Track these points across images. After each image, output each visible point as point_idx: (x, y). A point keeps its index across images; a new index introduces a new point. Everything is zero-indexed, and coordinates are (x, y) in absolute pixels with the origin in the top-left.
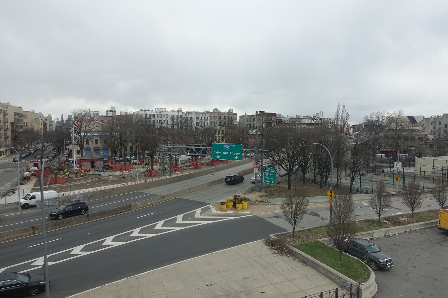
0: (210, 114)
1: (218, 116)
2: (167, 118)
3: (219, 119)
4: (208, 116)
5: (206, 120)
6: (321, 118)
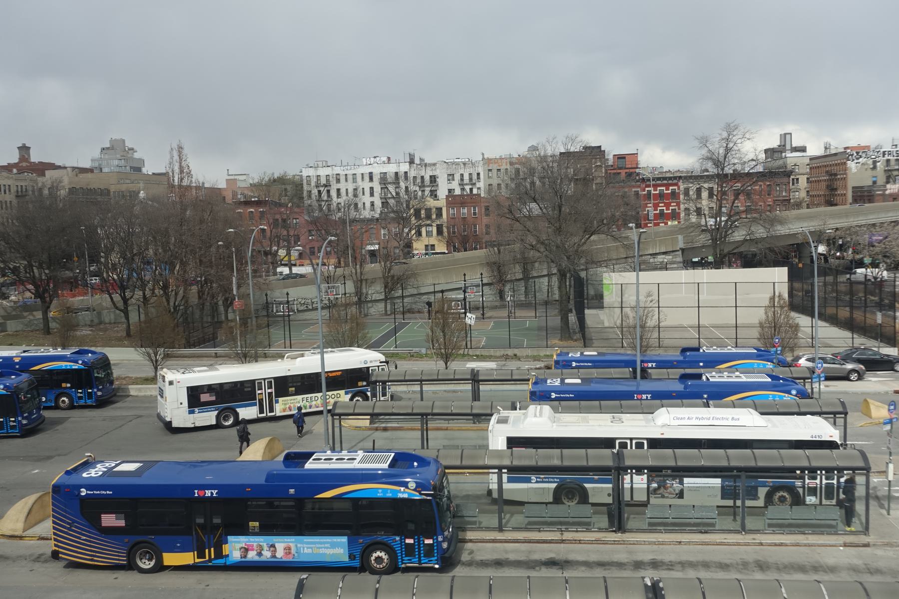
0: (486, 164)
1: (508, 167)
2: (371, 179)
3: (513, 176)
4: (480, 170)
5: (474, 182)
6: (884, 152)
